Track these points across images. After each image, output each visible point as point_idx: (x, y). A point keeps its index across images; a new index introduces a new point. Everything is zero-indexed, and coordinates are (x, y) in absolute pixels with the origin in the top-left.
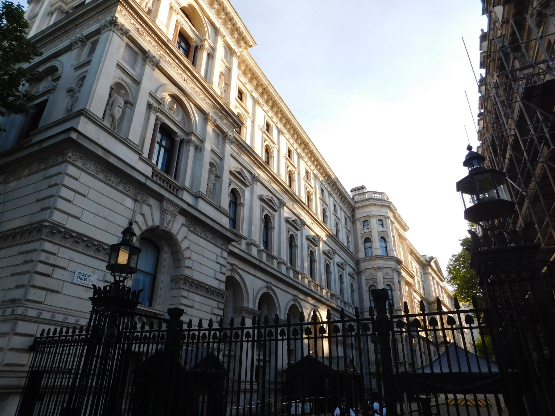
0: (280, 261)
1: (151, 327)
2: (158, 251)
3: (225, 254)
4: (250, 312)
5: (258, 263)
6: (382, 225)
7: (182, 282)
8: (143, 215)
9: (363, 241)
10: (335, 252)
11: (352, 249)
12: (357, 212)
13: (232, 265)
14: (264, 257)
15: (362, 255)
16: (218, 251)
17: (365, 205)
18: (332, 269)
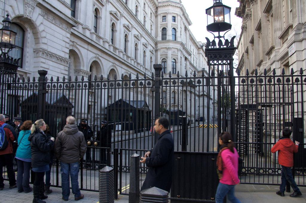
0: (104, 40)
1: (24, 81)
2: (23, 31)
3: (69, 35)
4: (85, 72)
5: (90, 41)
7: (41, 53)
8: (11, 6)
9: (161, 29)
10: (142, 36)
11: (153, 35)
12: (159, 9)
13: (73, 42)
14: (94, 38)
15: (160, 38)
16: (64, 33)
17: (165, 5)
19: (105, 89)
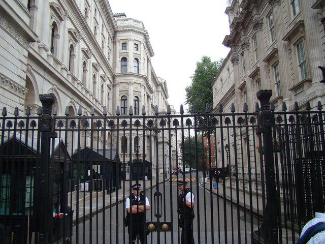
3: (26, 54)
6: (137, 48)
14: (52, 62)
15: (118, 71)
17: (126, 30)
18: (97, 80)
19: (228, 127)
